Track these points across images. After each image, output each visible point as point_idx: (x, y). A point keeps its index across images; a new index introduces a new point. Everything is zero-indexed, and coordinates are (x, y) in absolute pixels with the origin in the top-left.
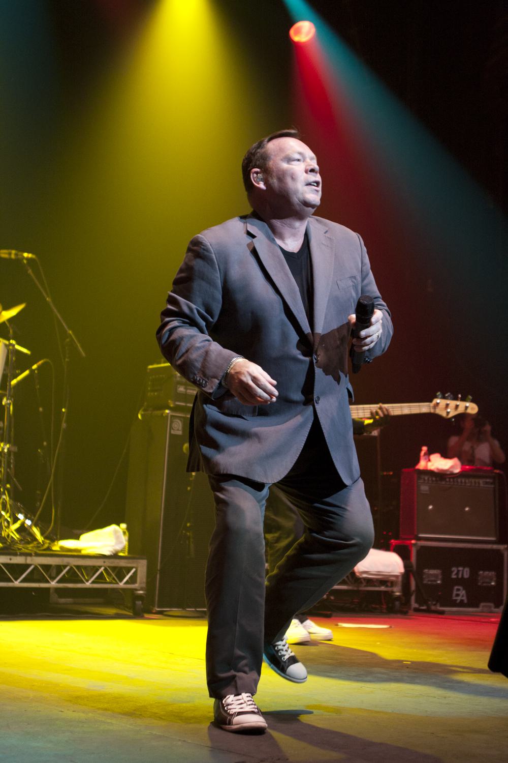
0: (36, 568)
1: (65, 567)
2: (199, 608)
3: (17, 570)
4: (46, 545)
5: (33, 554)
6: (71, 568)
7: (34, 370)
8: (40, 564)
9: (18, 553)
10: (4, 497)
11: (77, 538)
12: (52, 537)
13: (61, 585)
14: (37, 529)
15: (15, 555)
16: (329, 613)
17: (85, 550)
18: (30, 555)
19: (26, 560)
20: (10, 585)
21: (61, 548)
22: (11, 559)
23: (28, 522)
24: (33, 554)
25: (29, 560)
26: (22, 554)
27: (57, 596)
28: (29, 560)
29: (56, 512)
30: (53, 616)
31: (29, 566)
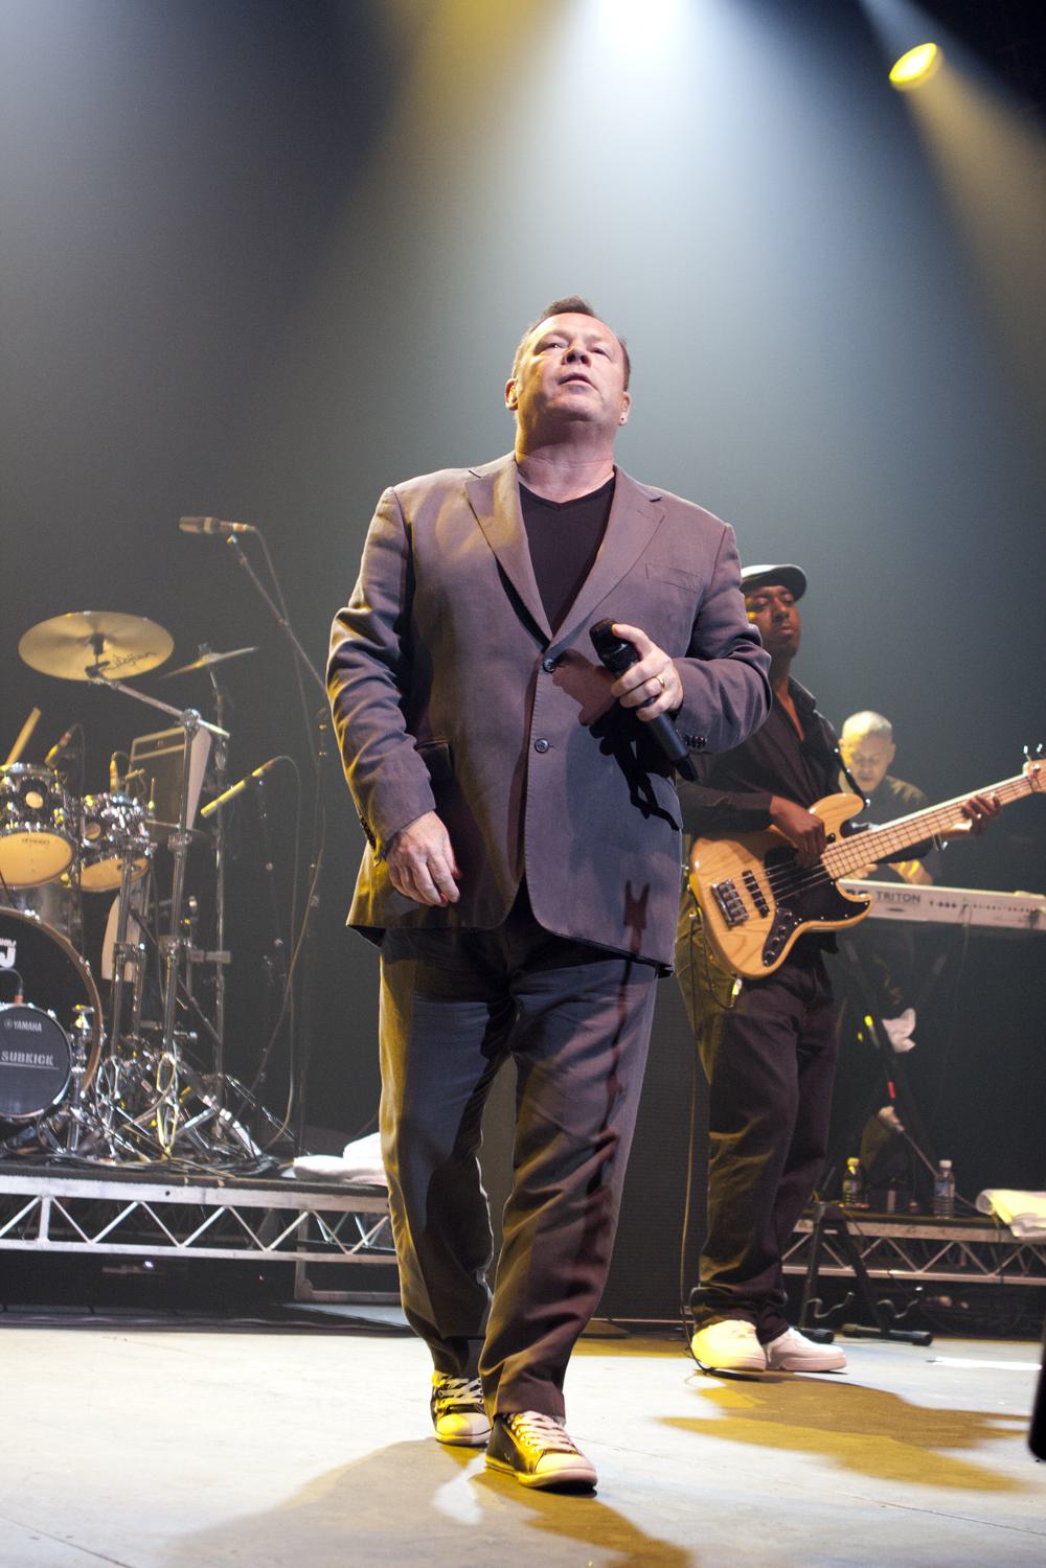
0: (227, 1213)
1: (304, 1211)
2: (615, 1317)
3: (183, 1219)
4: (265, 1166)
5: (221, 1183)
6: (311, 1219)
7: (257, 779)
8: (237, 1204)
9: (186, 1181)
10: (167, 1056)
11: (340, 1154)
12: (288, 1153)
13: (285, 1256)
14: (245, 1129)
15: (180, 1183)
16: (925, 1334)
17: (349, 1178)
18: (215, 1185)
19: (204, 1195)
20: (166, 1251)
21: (300, 1171)
22: (168, 1193)
23: (226, 1115)
24: (221, 1183)
25: (212, 1196)
26: (192, 1183)
27: (310, 1284)
28: (212, 1196)
29: (296, 1090)
30: (210, 1325)
31: (216, 1208)
